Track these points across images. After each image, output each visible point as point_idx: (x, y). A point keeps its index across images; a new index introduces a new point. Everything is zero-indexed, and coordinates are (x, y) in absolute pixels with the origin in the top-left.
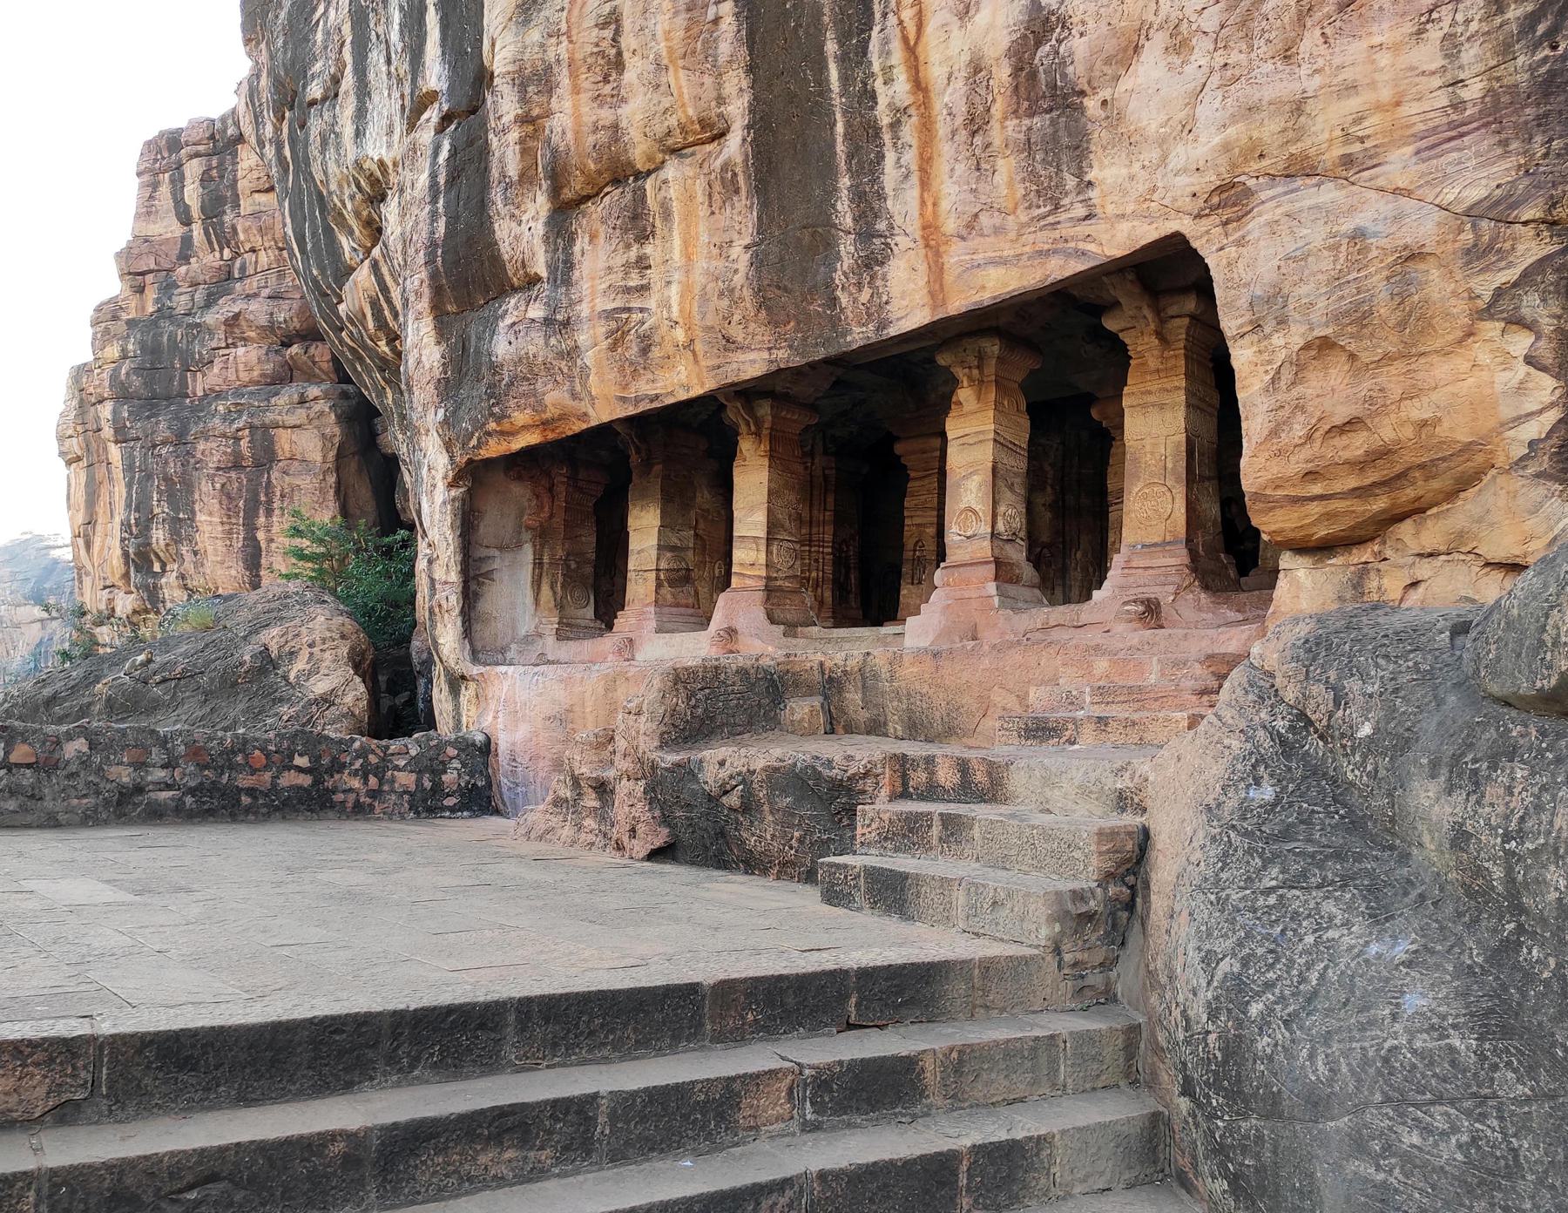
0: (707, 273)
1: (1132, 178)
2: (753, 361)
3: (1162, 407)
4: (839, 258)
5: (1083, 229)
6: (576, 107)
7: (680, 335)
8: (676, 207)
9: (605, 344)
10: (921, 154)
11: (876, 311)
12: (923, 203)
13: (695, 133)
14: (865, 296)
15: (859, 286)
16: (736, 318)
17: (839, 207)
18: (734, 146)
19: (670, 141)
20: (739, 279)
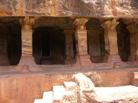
3: (114, 36)
11: (102, 12)
15: (98, 7)
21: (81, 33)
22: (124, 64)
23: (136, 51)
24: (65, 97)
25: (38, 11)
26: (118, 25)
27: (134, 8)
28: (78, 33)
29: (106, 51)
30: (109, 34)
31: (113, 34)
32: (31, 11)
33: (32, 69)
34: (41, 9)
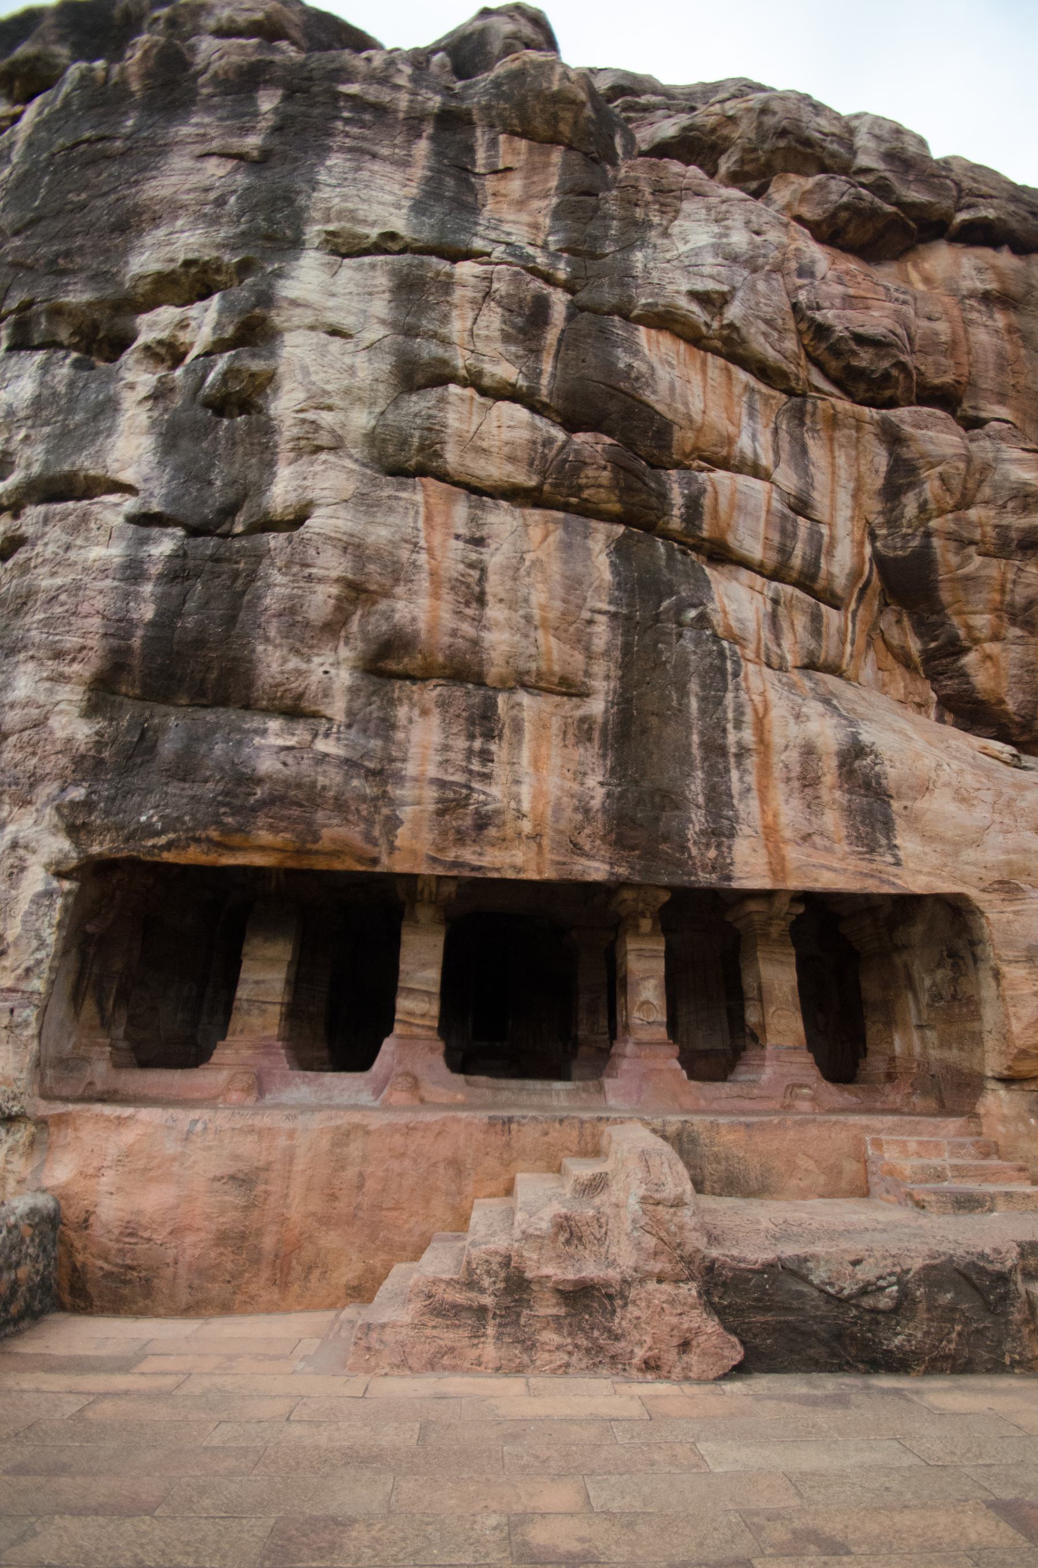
0: (561, 788)
1: (926, 854)
2: (597, 869)
3: (782, 963)
4: (691, 822)
5: (893, 869)
6: (434, 609)
7: (526, 826)
8: (528, 727)
9: (432, 807)
10: (759, 783)
11: (723, 867)
12: (763, 811)
13: (549, 682)
14: (712, 853)
15: (708, 846)
16: (587, 831)
17: (693, 787)
18: (597, 707)
19: (526, 678)
20: (596, 803)
21: (638, 946)
22: (834, 1094)
23: (891, 1037)
24: (565, 1224)
25: (473, 857)
26: (798, 916)
27: (860, 853)
28: (629, 947)
29: (751, 1030)
30: (758, 954)
31: (777, 957)
32: (451, 855)
33: (433, 1091)
34: (489, 850)
